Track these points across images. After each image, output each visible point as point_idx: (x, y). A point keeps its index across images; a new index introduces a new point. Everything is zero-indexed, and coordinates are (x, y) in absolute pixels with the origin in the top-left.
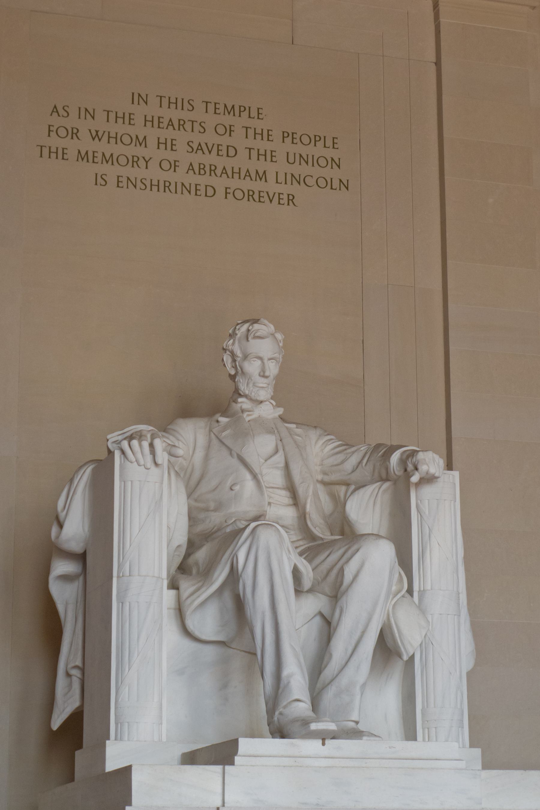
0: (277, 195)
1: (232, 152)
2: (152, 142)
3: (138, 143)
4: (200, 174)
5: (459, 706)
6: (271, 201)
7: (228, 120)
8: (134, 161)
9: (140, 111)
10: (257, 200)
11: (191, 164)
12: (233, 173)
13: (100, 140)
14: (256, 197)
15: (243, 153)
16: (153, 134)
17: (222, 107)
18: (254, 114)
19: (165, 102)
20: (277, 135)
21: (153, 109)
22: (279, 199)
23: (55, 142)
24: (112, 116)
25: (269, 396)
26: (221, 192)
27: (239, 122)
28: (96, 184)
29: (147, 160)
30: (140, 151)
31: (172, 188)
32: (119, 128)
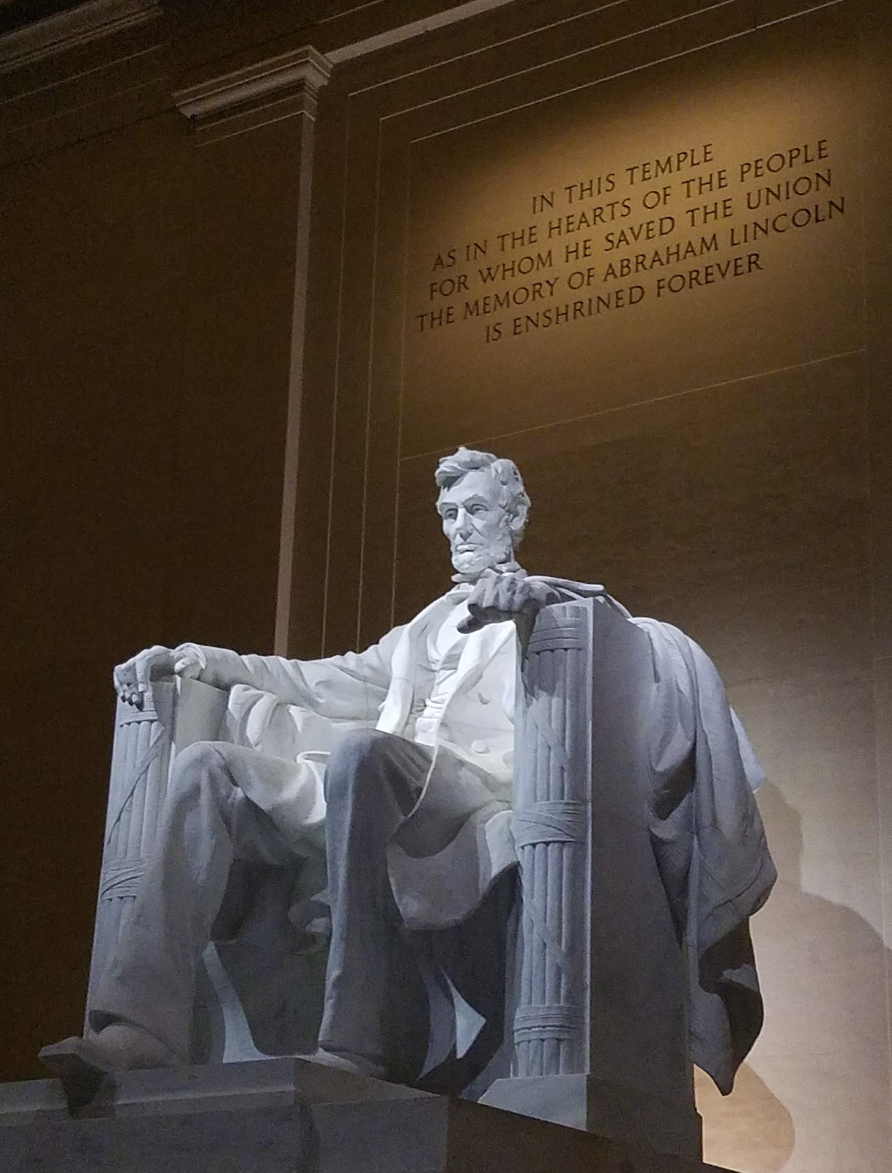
0: (732, 264)
1: (667, 224)
2: (559, 255)
3: (541, 265)
4: (622, 275)
6: (723, 275)
8: (536, 291)
10: (703, 281)
11: (611, 266)
12: (669, 255)
13: (493, 279)
16: (558, 245)
17: (652, 167)
18: (699, 157)
22: (736, 267)
27: (674, 179)
28: (488, 341)
29: (551, 282)
30: (544, 274)
31: (585, 310)
32: (519, 252)
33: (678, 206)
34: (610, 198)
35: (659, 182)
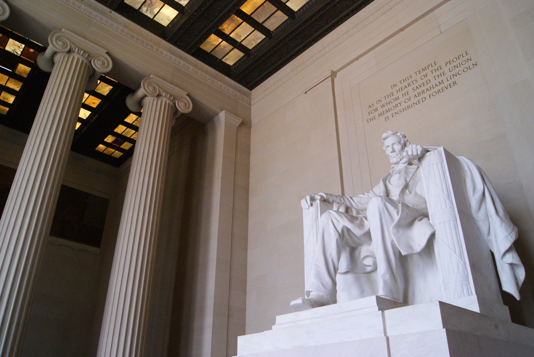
1: (428, 82)
2: (401, 97)
5: (461, 272)
7: (424, 73)
8: (396, 106)
9: (394, 90)
14: (441, 91)
15: (432, 80)
16: (400, 94)
17: (421, 70)
18: (433, 64)
19: (402, 82)
20: (443, 65)
21: (399, 86)
23: (372, 116)
24: (387, 97)
25: (399, 159)
26: (427, 97)
27: (428, 71)
31: (410, 107)
32: (390, 99)
33: (430, 76)
34: (412, 80)
35: (424, 73)
